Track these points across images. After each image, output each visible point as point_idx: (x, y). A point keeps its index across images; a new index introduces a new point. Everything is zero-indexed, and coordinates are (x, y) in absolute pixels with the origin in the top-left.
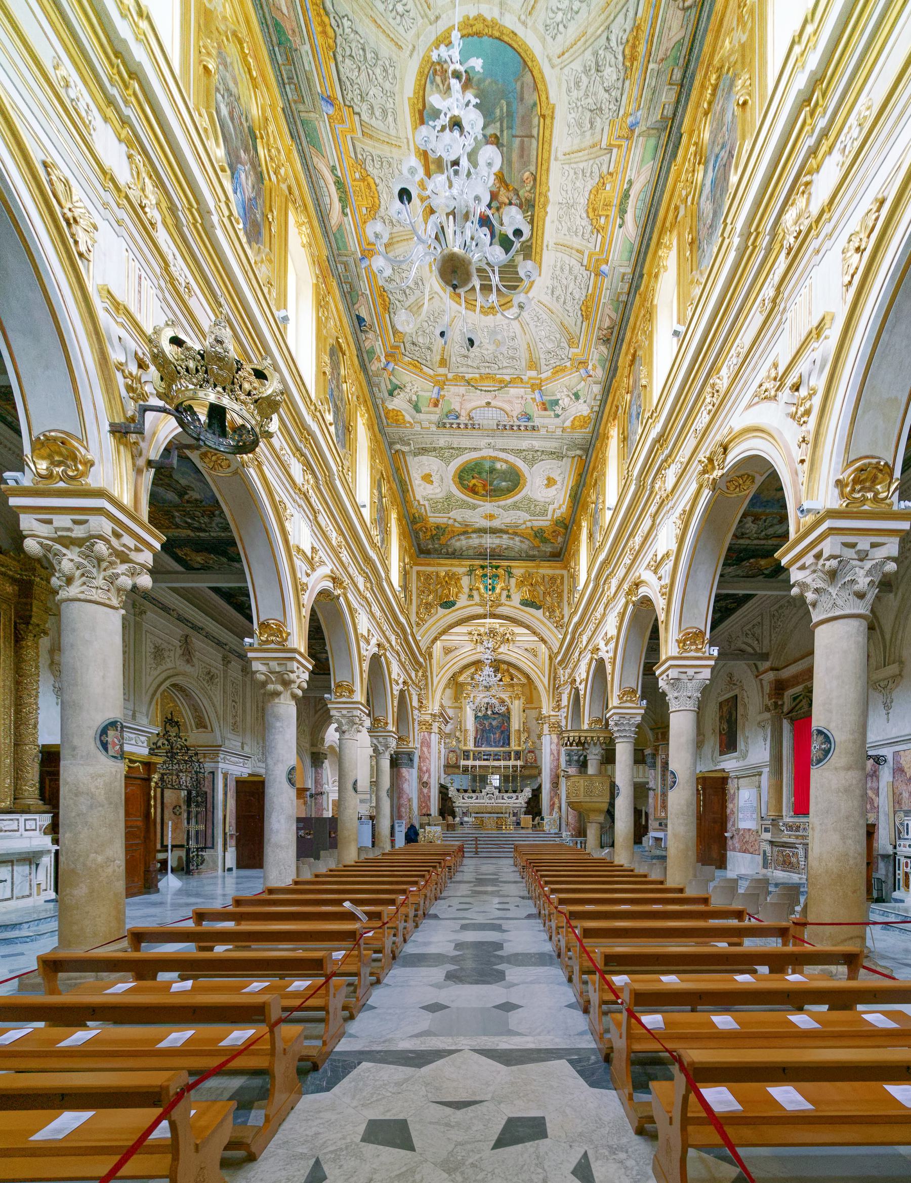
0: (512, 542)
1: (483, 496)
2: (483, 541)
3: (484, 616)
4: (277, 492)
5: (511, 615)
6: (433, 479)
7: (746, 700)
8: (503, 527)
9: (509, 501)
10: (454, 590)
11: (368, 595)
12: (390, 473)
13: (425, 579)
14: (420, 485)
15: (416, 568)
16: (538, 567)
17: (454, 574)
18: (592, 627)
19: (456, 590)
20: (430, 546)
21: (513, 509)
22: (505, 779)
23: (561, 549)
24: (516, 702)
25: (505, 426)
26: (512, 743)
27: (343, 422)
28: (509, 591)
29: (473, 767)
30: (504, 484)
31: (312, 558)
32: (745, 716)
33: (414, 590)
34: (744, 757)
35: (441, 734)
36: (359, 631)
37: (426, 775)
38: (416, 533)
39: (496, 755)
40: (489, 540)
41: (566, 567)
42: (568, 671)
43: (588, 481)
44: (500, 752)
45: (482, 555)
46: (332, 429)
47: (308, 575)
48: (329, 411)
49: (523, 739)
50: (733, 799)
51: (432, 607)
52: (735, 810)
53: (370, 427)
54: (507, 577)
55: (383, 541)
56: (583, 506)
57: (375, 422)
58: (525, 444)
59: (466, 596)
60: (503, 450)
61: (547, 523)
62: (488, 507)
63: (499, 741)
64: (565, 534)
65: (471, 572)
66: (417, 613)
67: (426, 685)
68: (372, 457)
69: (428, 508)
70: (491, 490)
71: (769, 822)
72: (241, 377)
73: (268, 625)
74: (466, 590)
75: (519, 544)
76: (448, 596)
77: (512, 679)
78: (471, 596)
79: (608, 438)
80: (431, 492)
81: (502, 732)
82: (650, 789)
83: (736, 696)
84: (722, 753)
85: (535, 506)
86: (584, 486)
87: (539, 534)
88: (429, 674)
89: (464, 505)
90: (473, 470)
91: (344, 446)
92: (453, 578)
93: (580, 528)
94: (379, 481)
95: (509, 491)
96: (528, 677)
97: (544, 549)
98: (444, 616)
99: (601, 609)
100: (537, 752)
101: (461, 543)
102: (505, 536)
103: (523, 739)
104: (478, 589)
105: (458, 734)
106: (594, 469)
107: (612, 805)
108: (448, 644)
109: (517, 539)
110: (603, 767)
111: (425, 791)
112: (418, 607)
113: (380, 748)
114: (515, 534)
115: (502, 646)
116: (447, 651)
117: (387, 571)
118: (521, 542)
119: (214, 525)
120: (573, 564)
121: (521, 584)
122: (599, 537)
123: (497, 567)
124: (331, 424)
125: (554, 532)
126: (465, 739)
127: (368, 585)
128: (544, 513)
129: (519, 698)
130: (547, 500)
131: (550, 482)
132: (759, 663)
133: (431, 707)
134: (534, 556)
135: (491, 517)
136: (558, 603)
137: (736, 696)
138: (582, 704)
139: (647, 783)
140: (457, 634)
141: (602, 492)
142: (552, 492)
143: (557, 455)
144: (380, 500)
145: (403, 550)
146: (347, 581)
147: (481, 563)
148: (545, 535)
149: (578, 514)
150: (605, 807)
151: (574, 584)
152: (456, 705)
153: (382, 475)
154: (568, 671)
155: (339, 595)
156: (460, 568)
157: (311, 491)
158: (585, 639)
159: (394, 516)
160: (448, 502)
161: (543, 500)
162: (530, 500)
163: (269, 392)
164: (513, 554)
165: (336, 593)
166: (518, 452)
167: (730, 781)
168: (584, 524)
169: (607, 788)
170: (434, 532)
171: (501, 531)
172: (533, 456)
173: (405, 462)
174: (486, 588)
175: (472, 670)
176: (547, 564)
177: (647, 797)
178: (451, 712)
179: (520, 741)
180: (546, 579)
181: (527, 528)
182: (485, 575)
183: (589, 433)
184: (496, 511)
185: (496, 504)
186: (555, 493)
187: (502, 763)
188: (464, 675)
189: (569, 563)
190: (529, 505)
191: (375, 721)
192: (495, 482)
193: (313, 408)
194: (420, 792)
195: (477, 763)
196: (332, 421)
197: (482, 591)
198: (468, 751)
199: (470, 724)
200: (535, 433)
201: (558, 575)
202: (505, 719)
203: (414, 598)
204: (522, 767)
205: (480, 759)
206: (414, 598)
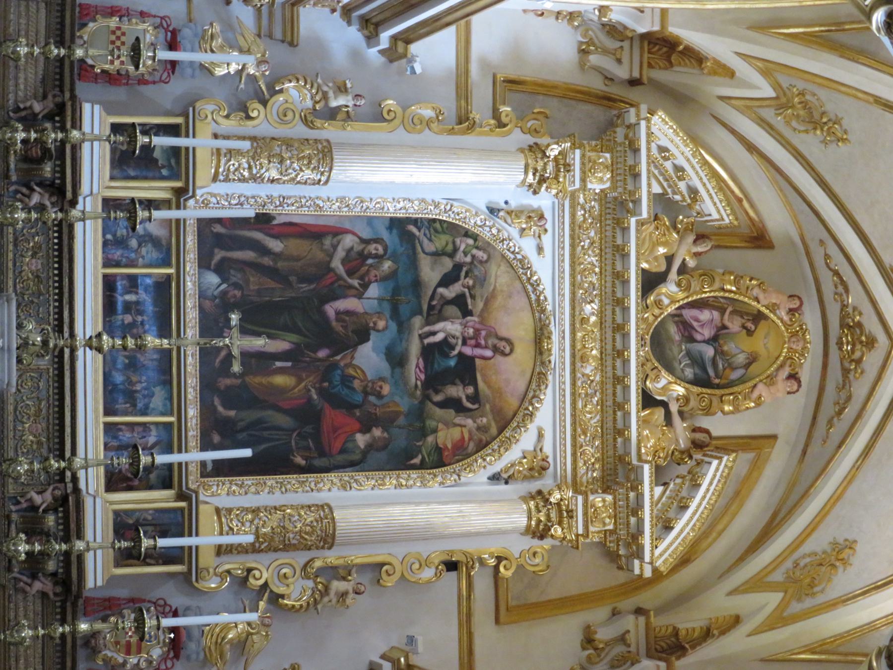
129: (540, 532)
202: (401, 440)
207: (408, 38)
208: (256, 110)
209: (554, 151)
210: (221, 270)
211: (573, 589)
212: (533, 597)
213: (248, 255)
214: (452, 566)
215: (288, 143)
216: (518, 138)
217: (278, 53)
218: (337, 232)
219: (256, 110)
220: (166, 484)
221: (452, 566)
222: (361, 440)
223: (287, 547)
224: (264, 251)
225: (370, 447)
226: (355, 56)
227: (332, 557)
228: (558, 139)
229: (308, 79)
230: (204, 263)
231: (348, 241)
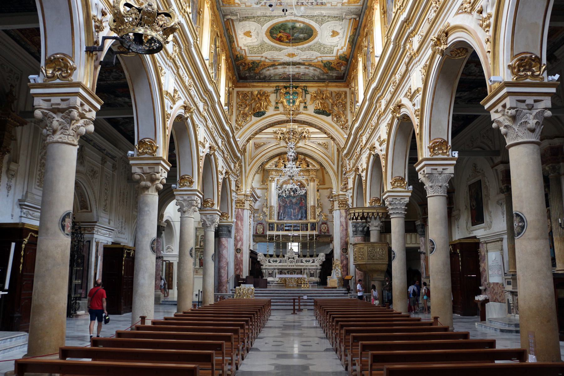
0: (307, 70)
1: (287, 43)
2: (286, 70)
3: (287, 121)
4: (158, 61)
5: (307, 121)
6: (252, 34)
7: (487, 184)
8: (301, 61)
9: (306, 45)
10: (264, 104)
11: (206, 115)
12: (223, 32)
13: (242, 97)
14: (242, 38)
15: (236, 89)
16: (327, 86)
17: (264, 93)
18: (369, 131)
19: (265, 104)
20: (247, 75)
21: (308, 50)
22: (304, 246)
23: (344, 74)
24: (312, 184)
25: (302, 3)
26: (309, 217)
27: (196, 9)
28: (305, 103)
29: (278, 236)
30: (301, 35)
31: (174, 96)
32: (488, 196)
33: (235, 105)
34: (490, 227)
35: (254, 211)
36: (199, 140)
37: (240, 244)
38: (238, 67)
39: (295, 226)
40: (291, 70)
41: (348, 85)
42: (352, 161)
43: (361, 32)
44: (298, 223)
45: (286, 78)
46: (191, 16)
47: (171, 108)
48: (189, 6)
49: (317, 213)
50: (484, 260)
51: (247, 116)
52: (486, 269)
53: (212, 8)
54: (304, 93)
55: (215, 76)
56: (359, 48)
57: (215, 4)
58: (316, 13)
59: (273, 108)
60: (301, 16)
61: (334, 58)
62: (290, 49)
63: (298, 215)
64: (347, 65)
65: (277, 91)
66: (236, 121)
67: (241, 172)
68: (212, 25)
69: (247, 51)
70: (293, 39)
71: (510, 277)
72: (158, 19)
73: (145, 142)
74: (273, 103)
75: (313, 71)
76: (259, 108)
77: (308, 166)
78: (277, 108)
79: (373, 9)
80: (250, 42)
81: (301, 208)
82: (421, 253)
83: (480, 181)
84: (473, 224)
85: (324, 48)
86: (358, 35)
87: (328, 66)
88: (243, 164)
89: (273, 48)
90: (280, 28)
91: (195, 23)
92: (264, 95)
93: (357, 61)
94: (216, 38)
95: (305, 39)
96: (321, 165)
97: (331, 74)
98: (255, 123)
99: (375, 119)
100: (329, 223)
101: (271, 71)
102: (302, 67)
103: (317, 213)
104: (282, 103)
105: (264, 209)
106: (365, 26)
107: (390, 266)
108: (257, 141)
109: (311, 68)
110: (383, 235)
111: (239, 255)
112: (237, 116)
113: (207, 223)
114: (310, 65)
115: (301, 141)
116: (257, 146)
117: (219, 96)
118: (314, 70)
119: (111, 77)
120: (353, 85)
121: (314, 98)
122: (371, 70)
123: (296, 87)
124: (190, 13)
125: (338, 63)
126: (270, 215)
127: (206, 108)
128: (331, 51)
129: (314, 180)
130: (332, 44)
131: (335, 34)
132: (494, 158)
133: (244, 190)
134: (324, 79)
135: (293, 55)
136: (343, 111)
137: (480, 181)
138: (364, 188)
139: (419, 248)
140: (266, 134)
141: (371, 41)
142: (336, 39)
143: (339, 18)
144: (215, 50)
145: (228, 79)
146: (193, 106)
147: (285, 84)
148: (332, 65)
149: (355, 53)
150: (385, 267)
151: (355, 98)
152: (264, 186)
153: (217, 34)
154: (352, 161)
155: (188, 117)
156: (269, 89)
157: (176, 57)
158: (364, 139)
159: (224, 58)
160: (262, 45)
161: (330, 44)
162: (320, 45)
163: (172, 24)
164: (308, 78)
165: (186, 116)
166: (312, 17)
167: (481, 245)
168: (360, 59)
169: (386, 252)
170: (251, 66)
171: (300, 64)
172: (321, 20)
173: (233, 25)
174: (288, 101)
175: (276, 159)
176: (334, 84)
177: (419, 259)
178: (259, 192)
179: (315, 215)
180: (334, 95)
181: (318, 61)
182: (288, 93)
183: (360, 5)
184: (296, 52)
185: (296, 47)
186: (338, 40)
187: (301, 233)
188: (270, 163)
189: (350, 84)
190: (320, 47)
191: (205, 202)
192: (295, 35)
193: (183, 11)
194: (236, 257)
195: (281, 233)
196: (191, 12)
197: (285, 103)
198: (273, 224)
199: (274, 201)
200: (323, 7)
201: (342, 92)
203: (234, 110)
204: (317, 236)
205: (282, 230)
206: (234, 110)
207: (258, 197)
208: (266, 214)
209: (270, 179)
210: (284, 218)
211: (321, 175)
212: (322, 180)
213: (282, 215)
214: (318, 191)
215: (270, 211)
216: (268, 183)
217: (260, 211)
218: (280, 204)
219: (266, 214)
220: (307, 224)
221: (318, 191)
222: (303, 201)
223: (315, 211)
224: (282, 213)
225: (304, 199)
226: (260, 202)
227: (316, 205)
228: (268, 178)
229: (263, 208)
230: (284, 220)
231: (281, 203)
